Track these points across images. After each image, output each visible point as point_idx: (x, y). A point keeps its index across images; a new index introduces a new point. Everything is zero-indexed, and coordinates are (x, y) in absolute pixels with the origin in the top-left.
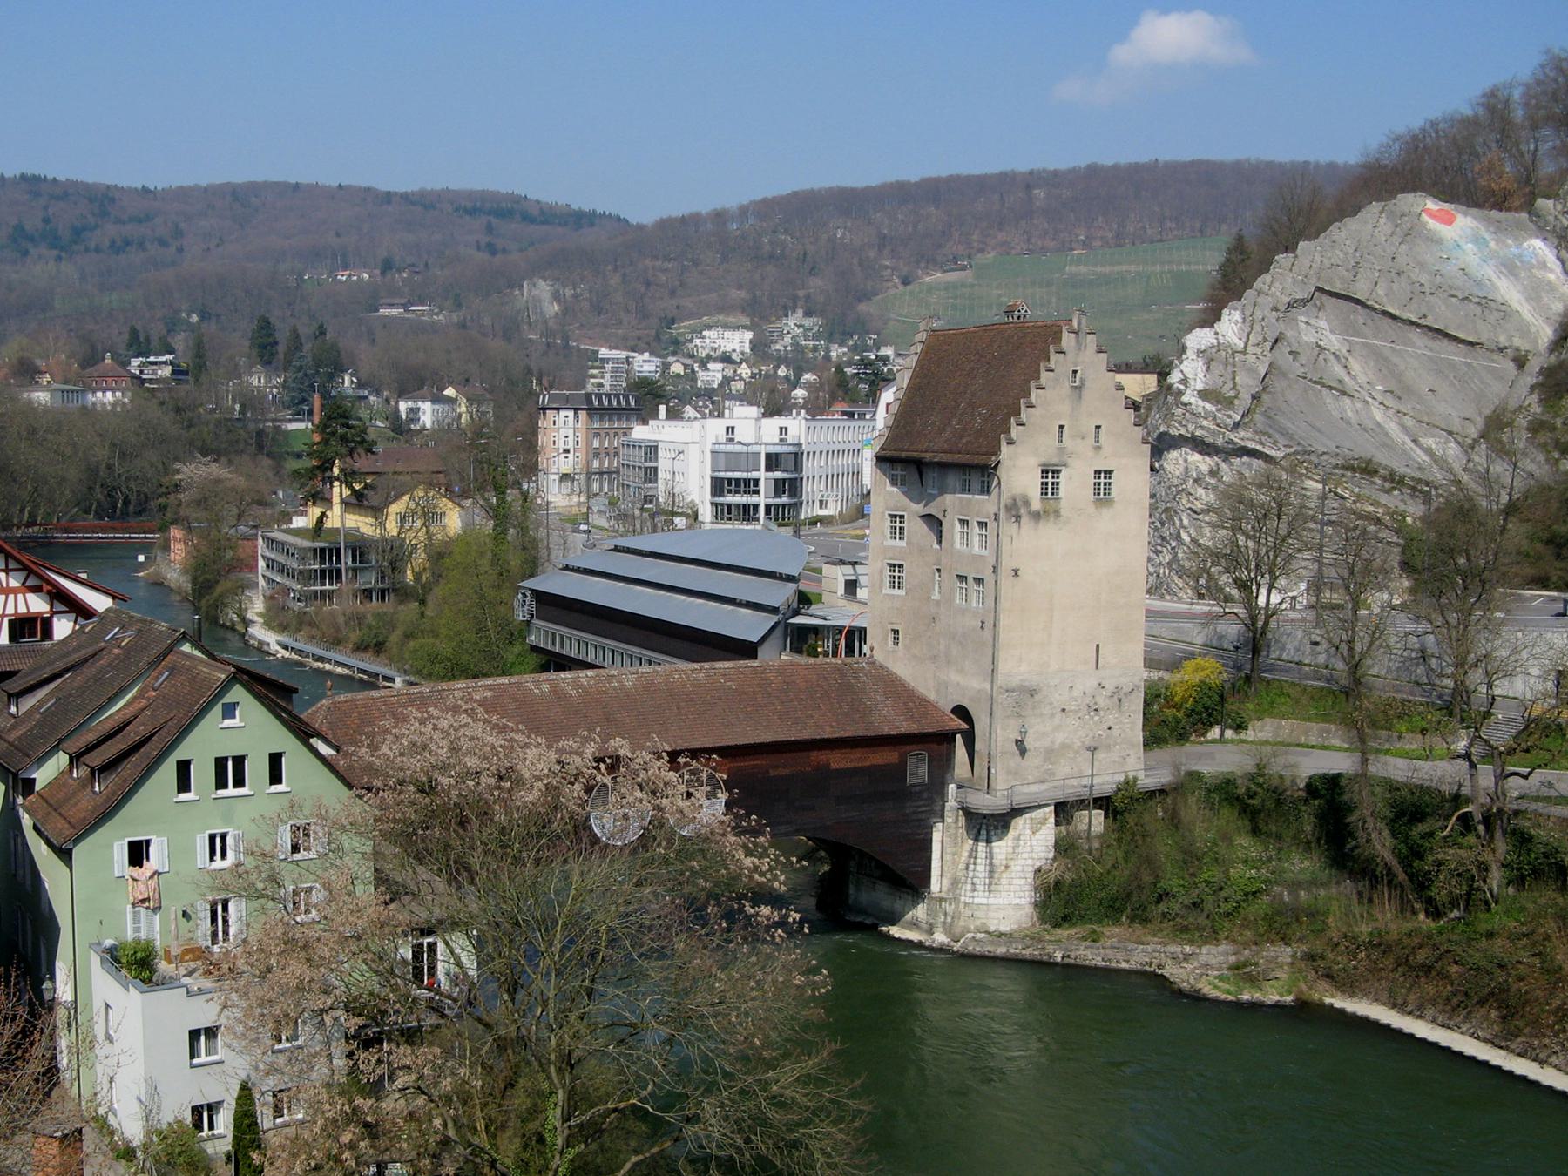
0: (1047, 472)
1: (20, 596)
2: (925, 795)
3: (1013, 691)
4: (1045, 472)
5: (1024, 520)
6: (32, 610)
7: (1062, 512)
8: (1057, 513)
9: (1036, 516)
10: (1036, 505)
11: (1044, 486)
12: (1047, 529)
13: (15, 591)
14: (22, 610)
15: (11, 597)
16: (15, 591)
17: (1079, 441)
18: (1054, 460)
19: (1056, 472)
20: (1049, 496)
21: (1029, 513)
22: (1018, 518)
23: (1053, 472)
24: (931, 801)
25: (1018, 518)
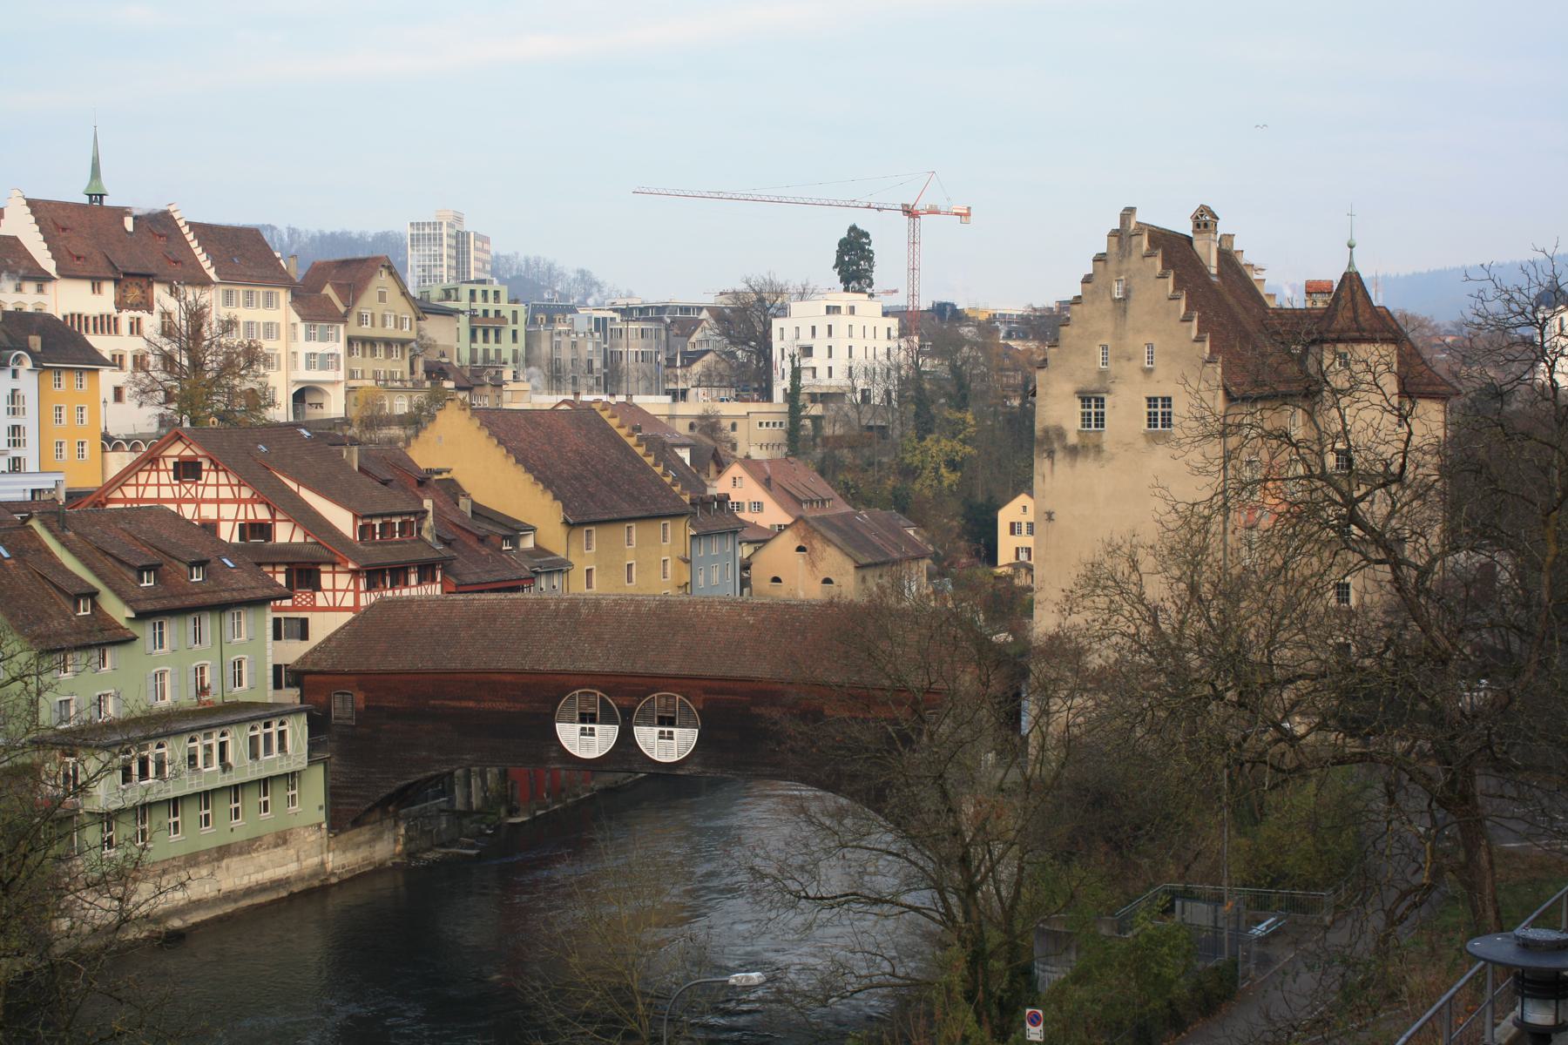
0: (1089, 401)
1: (249, 506)
5: (1059, 455)
6: (259, 518)
7: (1105, 447)
8: (1098, 449)
9: (1073, 452)
10: (1072, 439)
11: (1086, 418)
12: (1086, 468)
13: (245, 501)
14: (251, 516)
15: (242, 506)
16: (245, 501)
17: (1124, 363)
18: (1095, 386)
19: (1100, 402)
20: (1093, 428)
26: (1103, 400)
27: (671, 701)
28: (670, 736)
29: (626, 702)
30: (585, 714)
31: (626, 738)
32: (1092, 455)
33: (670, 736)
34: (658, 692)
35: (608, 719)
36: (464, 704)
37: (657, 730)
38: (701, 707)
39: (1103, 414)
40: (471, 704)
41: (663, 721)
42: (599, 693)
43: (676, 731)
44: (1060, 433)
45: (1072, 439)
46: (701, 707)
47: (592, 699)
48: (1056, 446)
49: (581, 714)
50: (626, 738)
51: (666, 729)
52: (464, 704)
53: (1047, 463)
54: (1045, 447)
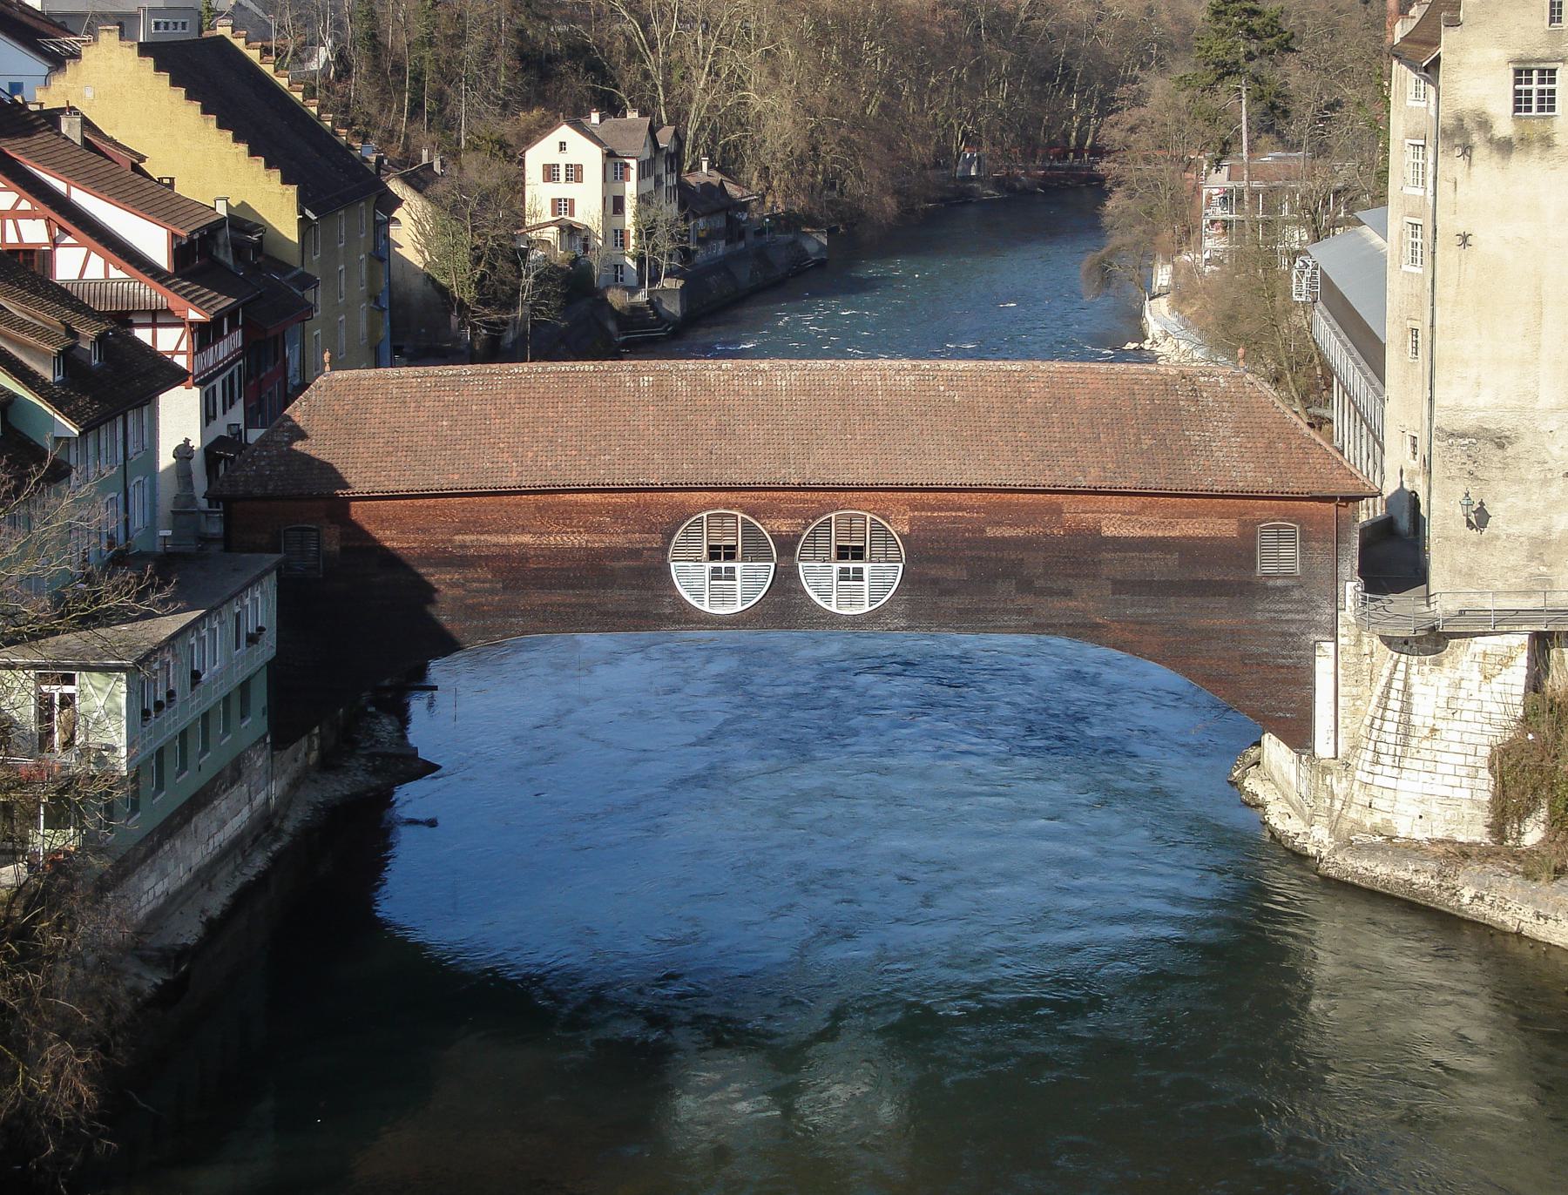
0: (1530, 72)
2: (1296, 594)
3: (1463, 436)
4: (1522, 74)
5: (1481, 152)
7: (1558, 139)
8: (1547, 142)
9: (1505, 147)
11: (1521, 102)
12: (1527, 169)
19: (1549, 75)
20: (1534, 112)
21: (1490, 141)
22: (1467, 149)
23: (1542, 72)
24: (1309, 605)
25: (1467, 149)
26: (1553, 72)
27: (857, 524)
28: (858, 575)
29: (784, 526)
30: (719, 547)
31: (786, 581)
32: (1536, 151)
33: (858, 575)
34: (837, 510)
35: (755, 550)
36: (514, 539)
37: (836, 566)
38: (906, 529)
39: (1552, 92)
40: (527, 539)
41: (843, 553)
42: (740, 515)
43: (867, 567)
44: (1484, 124)
45: (1504, 126)
46: (906, 529)
47: (729, 523)
48: (1476, 138)
49: (711, 547)
50: (786, 581)
51: (851, 565)
52: (514, 539)
53: (1461, 163)
54: (1457, 141)
